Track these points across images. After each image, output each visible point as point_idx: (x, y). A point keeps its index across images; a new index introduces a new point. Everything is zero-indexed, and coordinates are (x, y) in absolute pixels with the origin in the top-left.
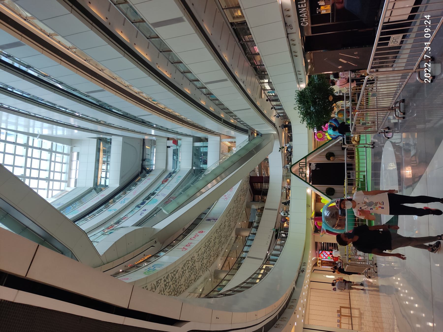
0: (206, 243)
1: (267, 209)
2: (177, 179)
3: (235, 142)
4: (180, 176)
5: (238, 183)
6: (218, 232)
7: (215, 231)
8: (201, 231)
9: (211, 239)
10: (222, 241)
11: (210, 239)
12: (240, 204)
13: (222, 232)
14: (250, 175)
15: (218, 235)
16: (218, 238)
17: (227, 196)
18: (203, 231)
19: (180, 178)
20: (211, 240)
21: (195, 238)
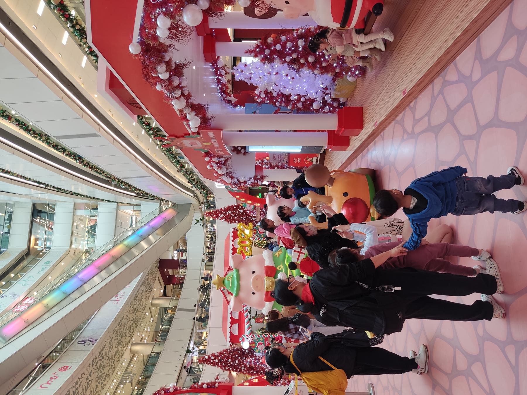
0: (69, 390)
1: (180, 310)
2: (42, 267)
3: (140, 211)
4: (49, 262)
5: (133, 280)
6: (95, 364)
8: (63, 368)
9: (80, 379)
10: (104, 373)
12: (141, 305)
14: (160, 258)
15: (97, 366)
17: (119, 296)
18: (67, 367)
19: (49, 265)
20: (81, 381)
21: (50, 384)
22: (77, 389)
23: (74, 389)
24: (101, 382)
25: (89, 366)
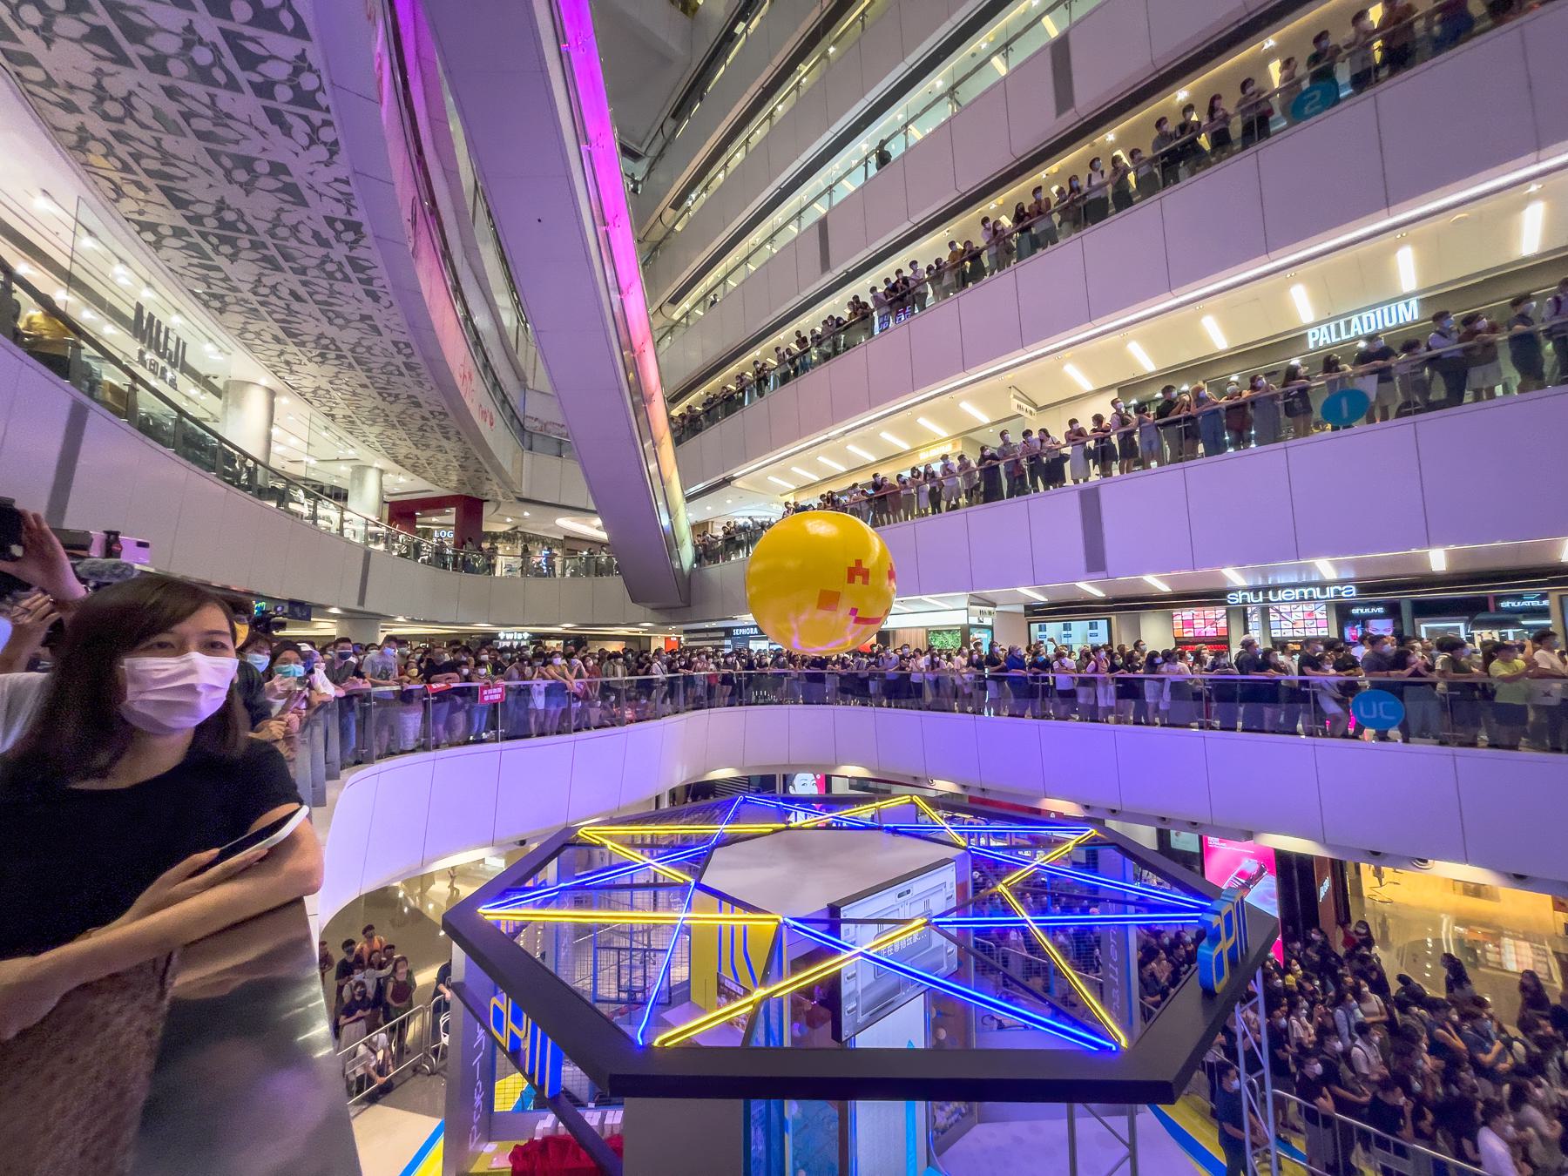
0: (300, 31)
7: (357, 216)
9: (315, 130)
11: (317, 117)
13: (305, 284)
16: (276, 223)
20: (300, 128)
22: (264, 89)
23: (277, 71)
24: (191, 228)
25: (347, 200)
